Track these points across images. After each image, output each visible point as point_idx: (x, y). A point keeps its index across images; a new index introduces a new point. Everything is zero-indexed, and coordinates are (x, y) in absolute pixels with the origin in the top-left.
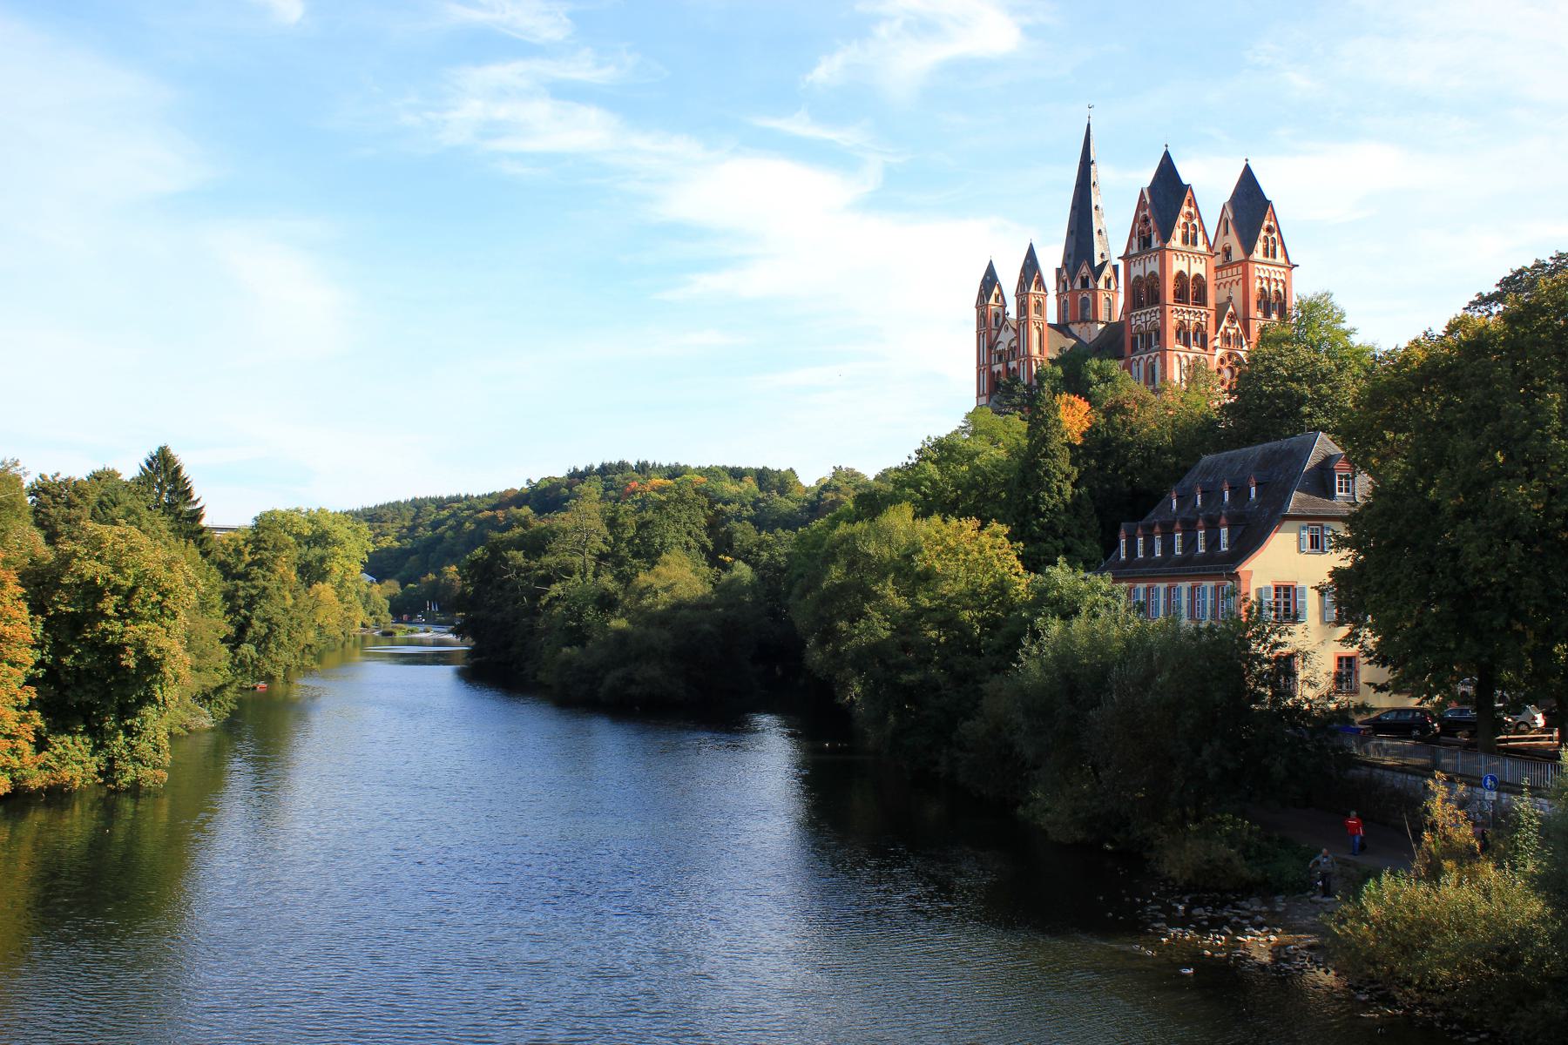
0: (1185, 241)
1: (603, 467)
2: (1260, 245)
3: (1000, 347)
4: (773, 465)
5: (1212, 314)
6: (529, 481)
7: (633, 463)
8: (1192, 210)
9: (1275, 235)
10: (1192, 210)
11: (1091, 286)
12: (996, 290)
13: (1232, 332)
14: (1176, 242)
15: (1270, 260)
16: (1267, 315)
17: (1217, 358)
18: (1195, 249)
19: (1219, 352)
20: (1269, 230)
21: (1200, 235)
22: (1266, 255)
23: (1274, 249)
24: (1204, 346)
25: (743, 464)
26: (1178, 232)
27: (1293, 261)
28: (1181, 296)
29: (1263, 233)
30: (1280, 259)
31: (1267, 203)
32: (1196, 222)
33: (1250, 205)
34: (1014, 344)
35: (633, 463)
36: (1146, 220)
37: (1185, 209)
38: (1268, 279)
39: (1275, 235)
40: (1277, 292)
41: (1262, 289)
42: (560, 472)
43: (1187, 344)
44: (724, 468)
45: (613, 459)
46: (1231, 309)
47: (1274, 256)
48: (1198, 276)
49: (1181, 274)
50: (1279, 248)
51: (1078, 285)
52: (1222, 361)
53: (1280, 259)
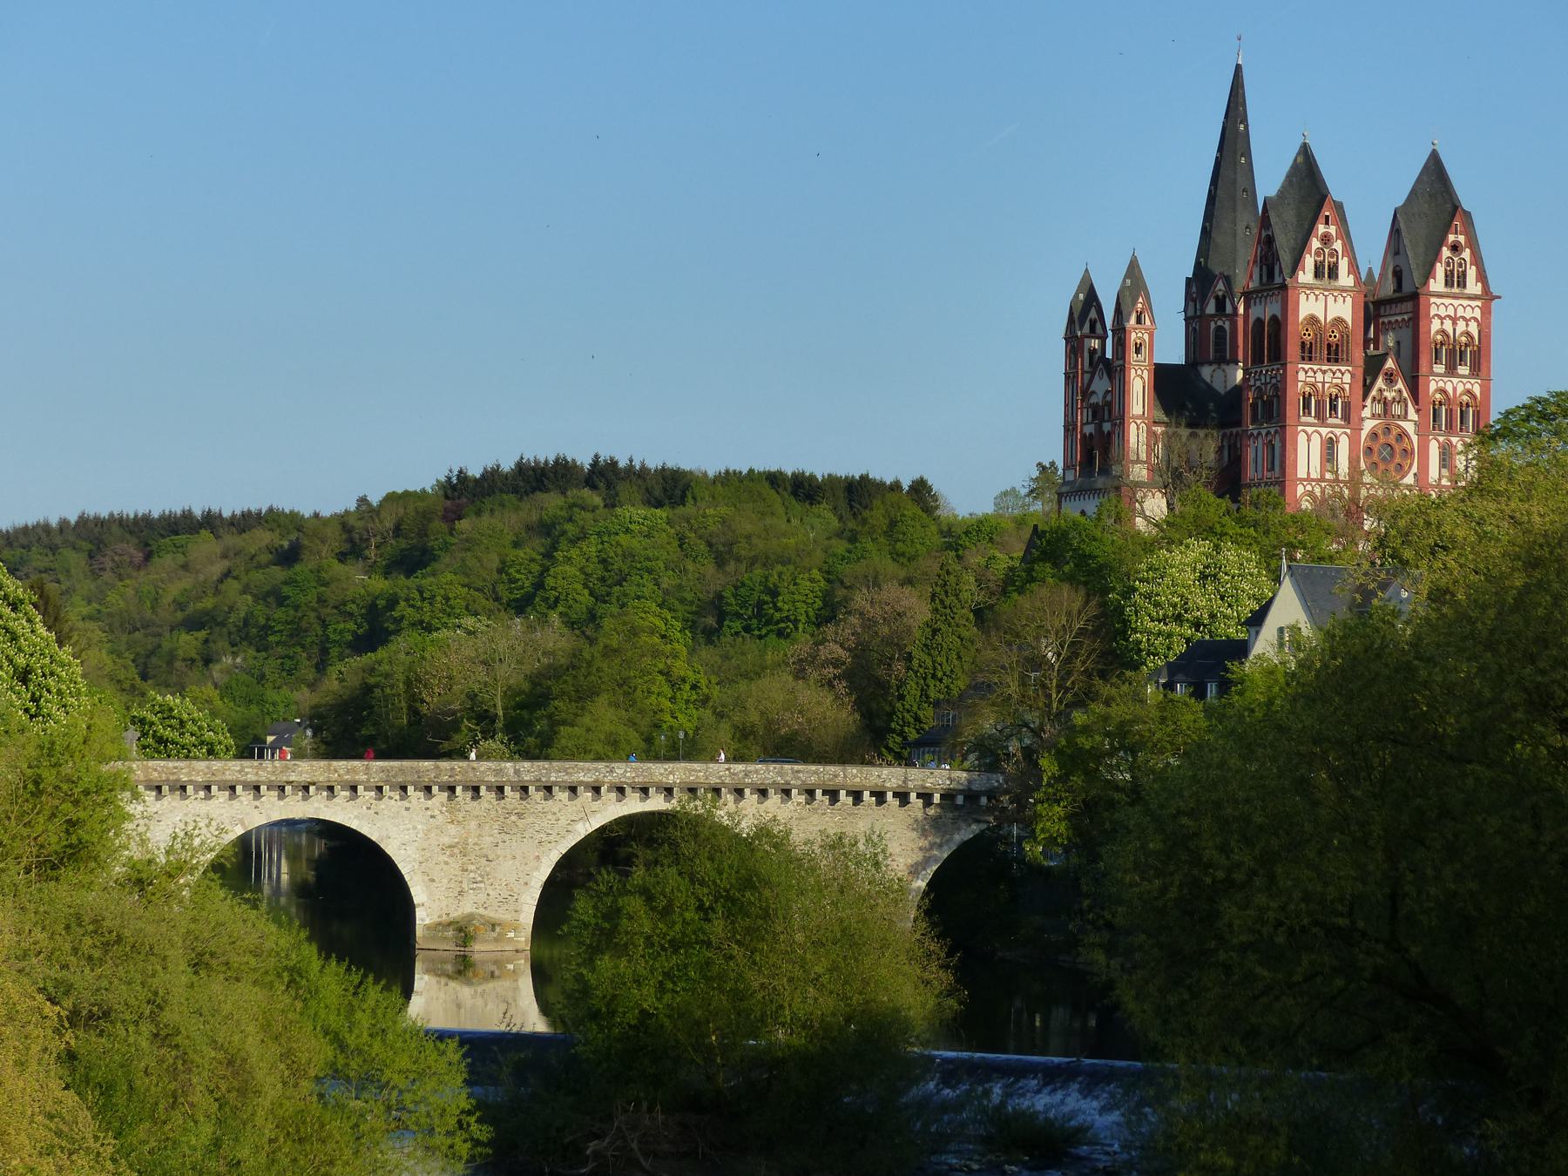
0: (1318, 273)
1: (521, 468)
2: (1440, 270)
3: (1093, 400)
4: (884, 473)
5: (1360, 373)
6: (363, 501)
7: (585, 461)
8: (1332, 230)
9: (1466, 254)
10: (1332, 230)
11: (1229, 309)
12: (1093, 314)
13: (1389, 395)
14: (1306, 276)
15: (1456, 290)
16: (1451, 371)
17: (1364, 434)
18: (1334, 284)
19: (1369, 425)
20: (1455, 248)
21: (1343, 265)
22: (1448, 282)
23: (1464, 274)
24: (1347, 417)
25: (819, 467)
26: (1309, 261)
27: (1494, 290)
28: (1308, 353)
29: (1446, 252)
30: (1473, 287)
31: (1455, 207)
32: (1338, 245)
33: (1434, 208)
34: (1109, 398)
35: (585, 461)
36: (1270, 241)
37: (1321, 228)
38: (1454, 320)
39: (1466, 254)
40: (1468, 334)
41: (1443, 332)
42: (423, 474)
43: (1317, 416)
44: (774, 479)
45: (543, 451)
46: (1390, 364)
47: (1462, 283)
48: (1339, 321)
49: (1313, 320)
50: (1472, 273)
51: (1211, 308)
52: (1374, 435)
53: (1473, 287)
